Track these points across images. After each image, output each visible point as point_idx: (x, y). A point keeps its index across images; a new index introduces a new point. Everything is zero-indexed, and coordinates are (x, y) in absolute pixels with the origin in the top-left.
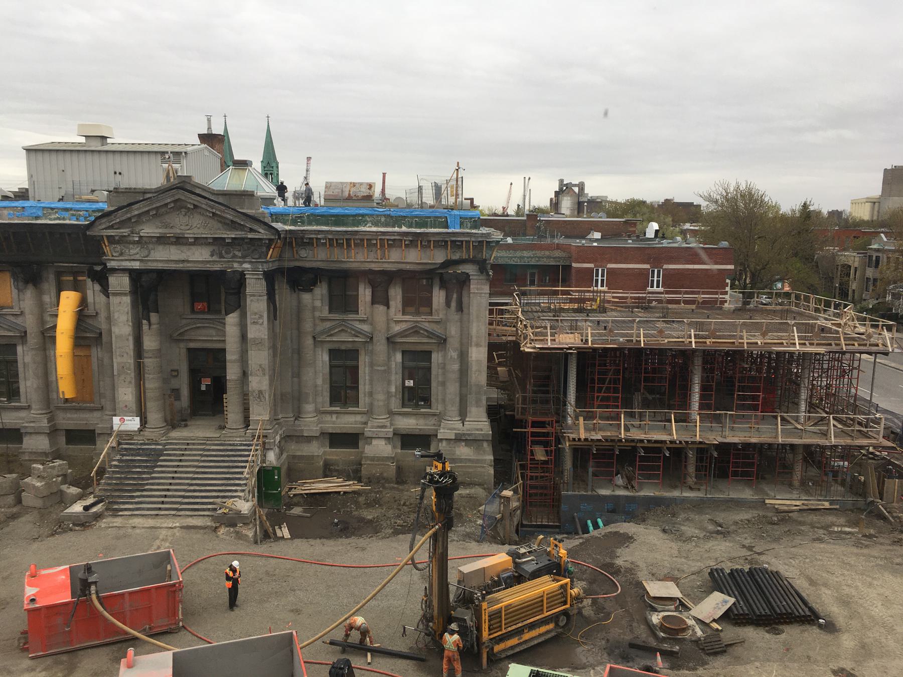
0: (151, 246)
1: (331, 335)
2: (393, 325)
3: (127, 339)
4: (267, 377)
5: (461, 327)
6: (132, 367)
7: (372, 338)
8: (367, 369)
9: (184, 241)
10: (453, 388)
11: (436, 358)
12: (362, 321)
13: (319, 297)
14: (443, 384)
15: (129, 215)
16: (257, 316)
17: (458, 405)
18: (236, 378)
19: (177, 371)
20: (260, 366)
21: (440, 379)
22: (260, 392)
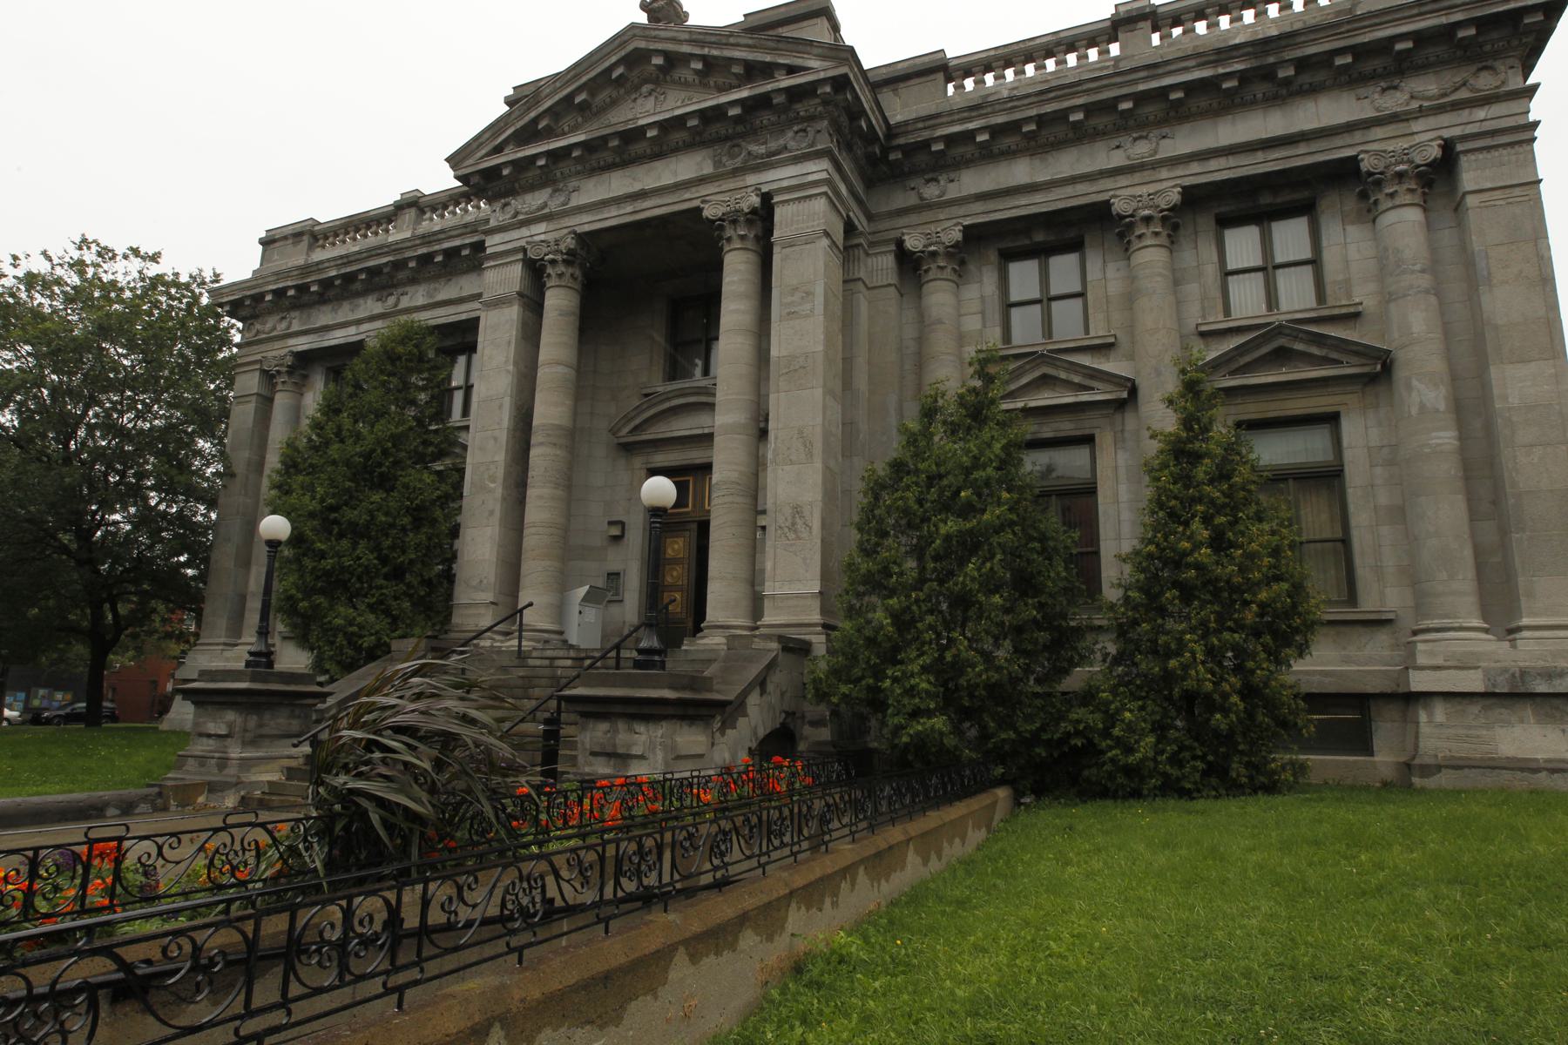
0: (573, 184)
1: (1011, 395)
2: (1197, 346)
3: (501, 407)
4: (818, 465)
5: (1441, 304)
6: (500, 473)
7: (1133, 391)
8: (1123, 488)
9: (638, 148)
10: (1445, 516)
11: (1360, 433)
12: (1105, 348)
13: (975, 306)
14: (1400, 514)
15: (533, 114)
16: (797, 297)
17: (1471, 573)
18: (734, 476)
19: (622, 524)
20: (801, 432)
21: (1383, 499)
22: (797, 510)
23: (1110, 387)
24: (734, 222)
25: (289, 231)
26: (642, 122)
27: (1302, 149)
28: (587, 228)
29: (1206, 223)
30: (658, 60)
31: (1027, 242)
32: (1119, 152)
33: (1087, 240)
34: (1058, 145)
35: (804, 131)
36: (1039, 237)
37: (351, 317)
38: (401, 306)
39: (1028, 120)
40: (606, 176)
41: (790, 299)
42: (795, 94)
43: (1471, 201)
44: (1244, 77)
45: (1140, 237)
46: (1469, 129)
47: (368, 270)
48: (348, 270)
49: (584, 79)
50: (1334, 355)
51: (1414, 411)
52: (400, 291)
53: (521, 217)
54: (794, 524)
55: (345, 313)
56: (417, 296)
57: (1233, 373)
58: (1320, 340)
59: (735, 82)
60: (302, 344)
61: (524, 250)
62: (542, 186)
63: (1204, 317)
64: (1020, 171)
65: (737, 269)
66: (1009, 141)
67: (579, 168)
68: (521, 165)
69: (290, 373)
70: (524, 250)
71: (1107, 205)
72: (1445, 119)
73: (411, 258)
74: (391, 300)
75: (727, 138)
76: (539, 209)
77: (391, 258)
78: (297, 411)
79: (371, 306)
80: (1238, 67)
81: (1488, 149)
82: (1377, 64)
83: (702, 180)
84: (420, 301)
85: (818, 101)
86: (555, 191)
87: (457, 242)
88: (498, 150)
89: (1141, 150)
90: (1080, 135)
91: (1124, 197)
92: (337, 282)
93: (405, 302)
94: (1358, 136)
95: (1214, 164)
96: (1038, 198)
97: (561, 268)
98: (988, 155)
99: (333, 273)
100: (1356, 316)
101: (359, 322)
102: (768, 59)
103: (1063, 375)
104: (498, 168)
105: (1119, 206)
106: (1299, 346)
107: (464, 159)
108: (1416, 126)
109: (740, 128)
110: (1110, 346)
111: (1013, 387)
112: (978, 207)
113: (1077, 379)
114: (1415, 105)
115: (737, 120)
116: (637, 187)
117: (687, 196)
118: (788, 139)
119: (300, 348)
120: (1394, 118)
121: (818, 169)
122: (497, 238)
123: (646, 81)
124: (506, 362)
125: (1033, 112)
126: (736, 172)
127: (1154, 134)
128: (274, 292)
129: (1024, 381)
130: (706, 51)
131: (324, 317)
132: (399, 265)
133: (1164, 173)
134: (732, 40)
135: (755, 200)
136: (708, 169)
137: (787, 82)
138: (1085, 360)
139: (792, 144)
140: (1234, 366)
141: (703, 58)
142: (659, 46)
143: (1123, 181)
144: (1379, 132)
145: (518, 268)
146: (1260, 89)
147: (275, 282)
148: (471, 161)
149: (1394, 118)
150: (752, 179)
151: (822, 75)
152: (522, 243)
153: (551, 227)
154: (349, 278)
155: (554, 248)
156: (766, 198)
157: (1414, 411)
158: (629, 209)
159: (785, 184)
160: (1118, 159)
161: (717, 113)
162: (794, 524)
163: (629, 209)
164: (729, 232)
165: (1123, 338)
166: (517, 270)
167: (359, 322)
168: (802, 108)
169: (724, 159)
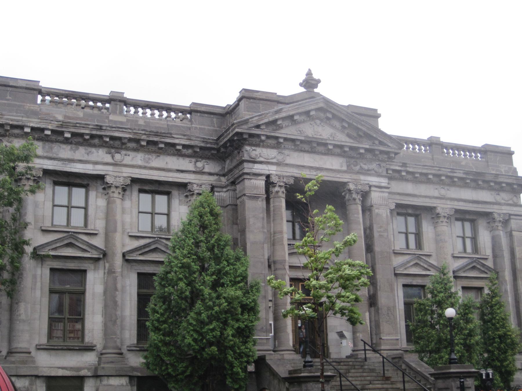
0: (286, 152)
1: (405, 269)
3: (263, 248)
9: (321, 149)
15: (277, 117)
16: (382, 229)
23: (435, 271)
24: (358, 193)
25: (24, 85)
26: (328, 142)
27: (480, 206)
28: (296, 175)
29: (453, 219)
30: (330, 116)
31: (405, 212)
32: (436, 191)
33: (423, 216)
34: (421, 182)
35: (379, 165)
36: (410, 211)
37: (86, 158)
38: (124, 162)
39: (417, 173)
40: (301, 154)
41: (379, 230)
42: (382, 152)
43: (514, 233)
44: (472, 180)
45: (442, 222)
46: (512, 213)
47: (112, 138)
48: (98, 133)
49: (300, 111)
50: (486, 271)
51: (503, 290)
52: (123, 152)
53: (261, 159)
54: (388, 314)
55: (81, 153)
56: (138, 158)
57: (464, 272)
58: (483, 265)
59: (355, 135)
60: (50, 165)
61: (268, 177)
62: (273, 147)
63: (454, 251)
64: (409, 188)
65: (356, 210)
66: (409, 177)
67: (293, 147)
68: (268, 137)
69: (34, 180)
70: (268, 177)
71: (435, 208)
72: (508, 208)
73: (143, 140)
74: (118, 157)
75: (353, 158)
76: (272, 159)
77: (131, 136)
78: (36, 205)
79: (101, 154)
80: (471, 177)
81: (516, 219)
82: (497, 187)
83: (345, 172)
84: (140, 163)
85: (386, 156)
86: (279, 153)
87: (177, 141)
88: (258, 127)
89: (443, 192)
90: (428, 182)
91: (444, 208)
92: (87, 137)
93: (128, 160)
94: (491, 206)
95: (461, 203)
96: (415, 199)
97: (283, 189)
98: (402, 179)
99: (87, 132)
100: (486, 259)
101: (96, 163)
102: (374, 136)
103: (422, 264)
104: (258, 136)
105: (439, 210)
106: (478, 266)
107: (242, 125)
108: (504, 207)
109: (358, 156)
110: (430, 255)
111: (408, 265)
112: (398, 197)
113: (426, 266)
114: (503, 201)
115: (361, 154)
116: (316, 165)
117: (338, 176)
118: (374, 166)
119: (45, 167)
120: (499, 204)
121: (384, 182)
122: (250, 165)
123: (318, 118)
124: (263, 227)
125: (420, 171)
126: (358, 173)
127: (446, 188)
128: (33, 129)
129: (412, 263)
130: (351, 122)
131: (65, 151)
132: (130, 140)
133: (448, 202)
134: (362, 123)
135: (367, 189)
136: (345, 168)
137: (382, 148)
138: (424, 258)
139: (376, 169)
140: (464, 270)
141: (349, 124)
142: (333, 111)
143: (438, 201)
144: (496, 207)
145: (264, 182)
146: (473, 184)
147: (37, 123)
148: (245, 127)
149: (499, 204)
150: (362, 177)
151: (393, 150)
152: (268, 173)
153: (279, 169)
154: (92, 136)
155: (282, 180)
156: (370, 187)
157: (503, 290)
158: (315, 173)
159: (374, 184)
160: (436, 194)
161: (357, 149)
162: (388, 314)
163: (315, 173)
164: (354, 196)
165: (434, 254)
166: (261, 183)
167: (96, 163)
168: (381, 157)
169: (352, 166)
